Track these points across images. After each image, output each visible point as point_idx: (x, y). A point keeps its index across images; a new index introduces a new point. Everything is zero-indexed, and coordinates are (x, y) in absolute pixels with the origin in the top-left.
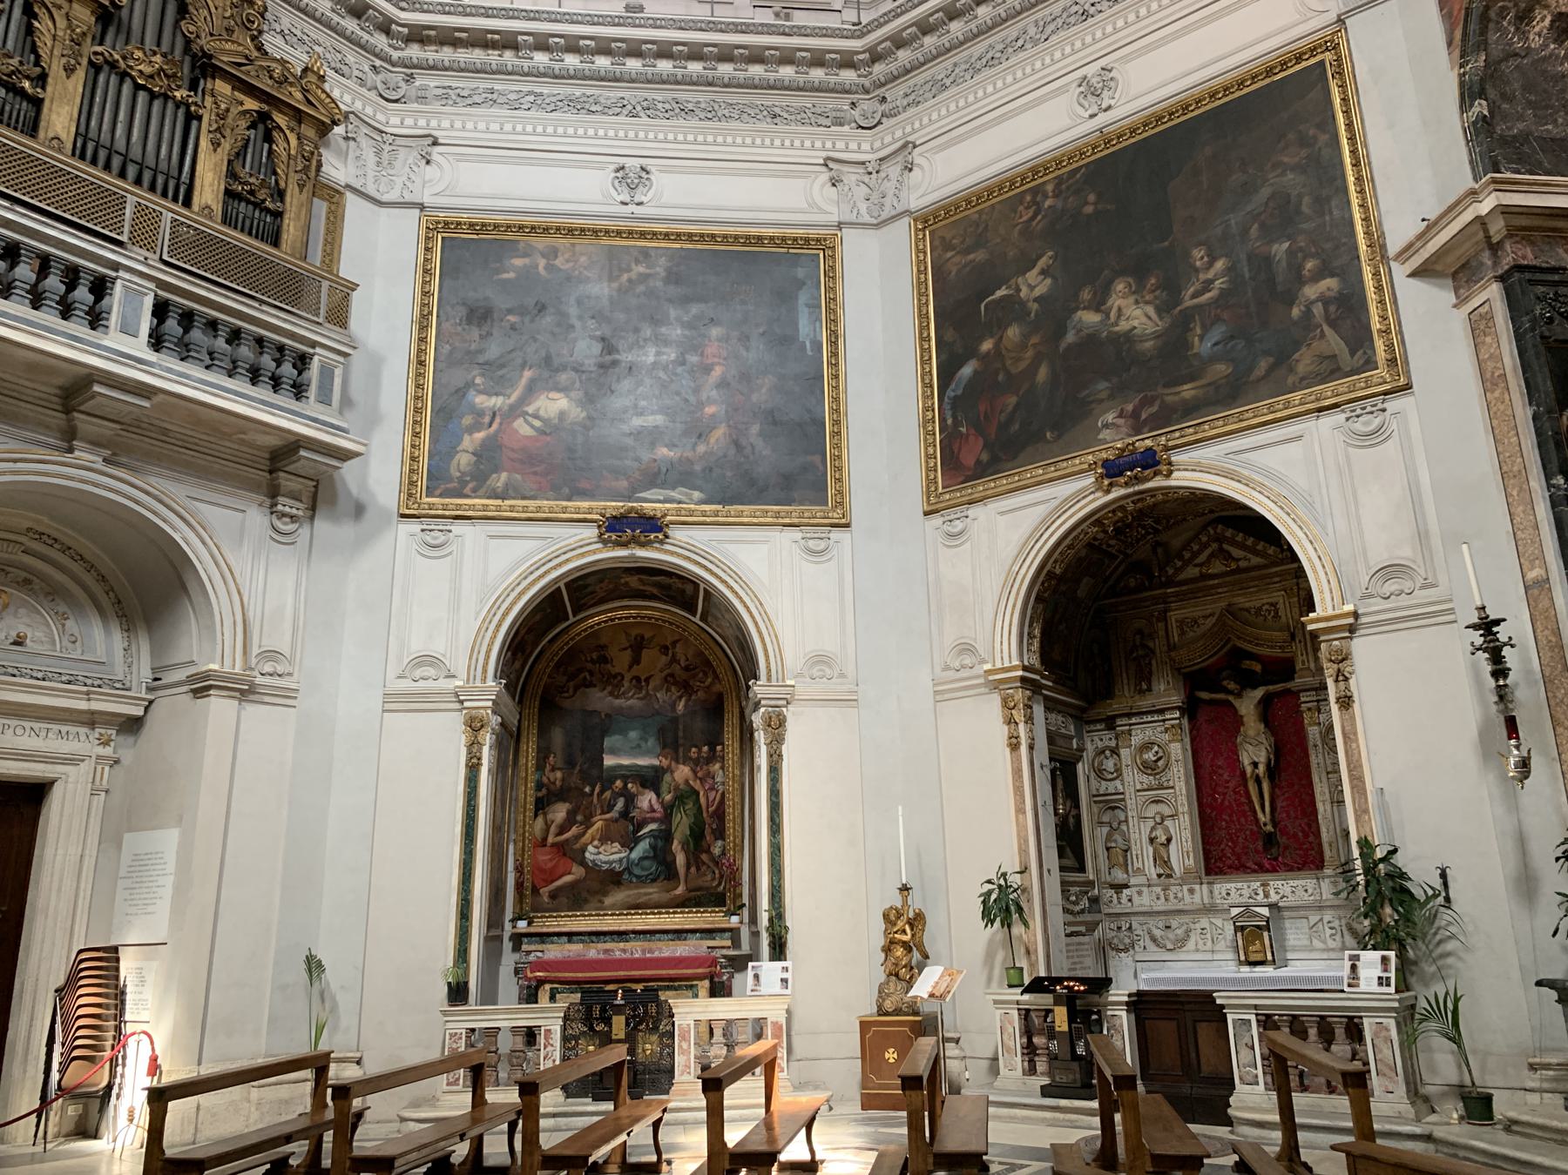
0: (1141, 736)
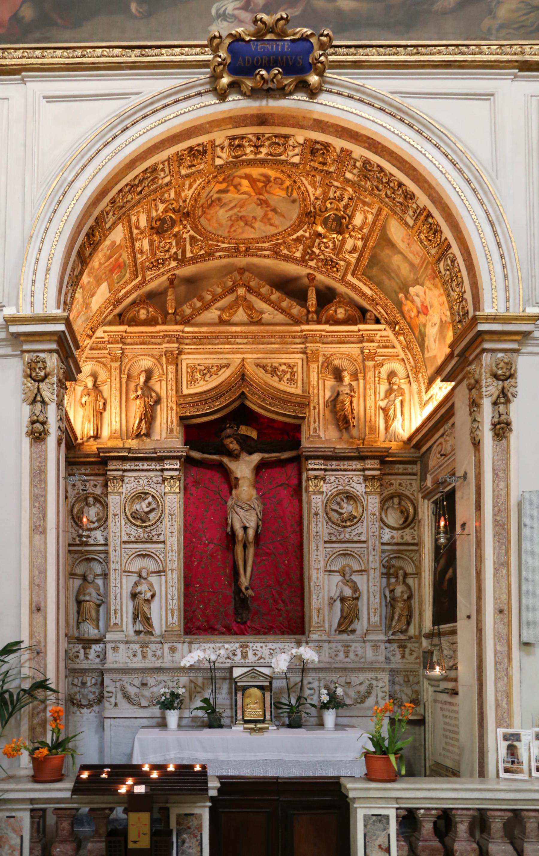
0: (134, 485)
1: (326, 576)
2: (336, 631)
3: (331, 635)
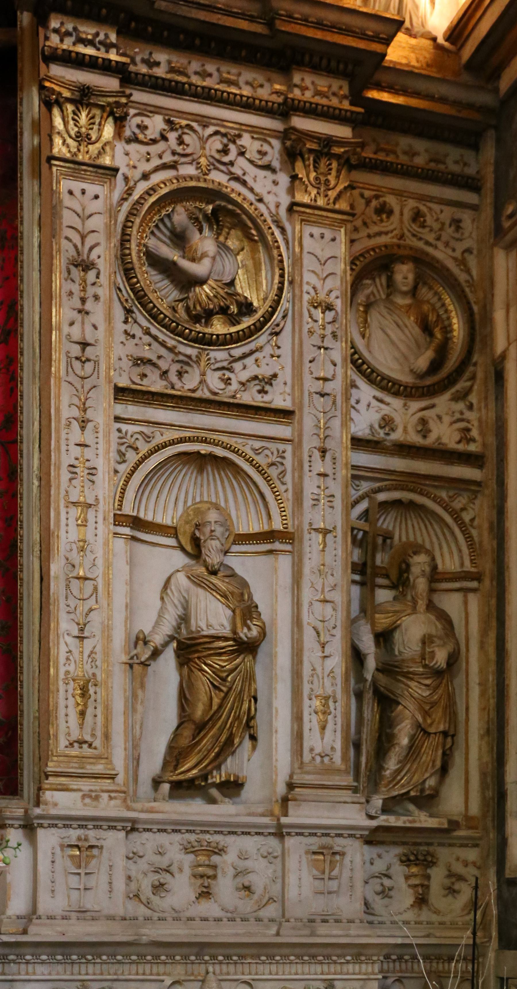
1: (120, 544)
2: (156, 783)
3: (135, 798)
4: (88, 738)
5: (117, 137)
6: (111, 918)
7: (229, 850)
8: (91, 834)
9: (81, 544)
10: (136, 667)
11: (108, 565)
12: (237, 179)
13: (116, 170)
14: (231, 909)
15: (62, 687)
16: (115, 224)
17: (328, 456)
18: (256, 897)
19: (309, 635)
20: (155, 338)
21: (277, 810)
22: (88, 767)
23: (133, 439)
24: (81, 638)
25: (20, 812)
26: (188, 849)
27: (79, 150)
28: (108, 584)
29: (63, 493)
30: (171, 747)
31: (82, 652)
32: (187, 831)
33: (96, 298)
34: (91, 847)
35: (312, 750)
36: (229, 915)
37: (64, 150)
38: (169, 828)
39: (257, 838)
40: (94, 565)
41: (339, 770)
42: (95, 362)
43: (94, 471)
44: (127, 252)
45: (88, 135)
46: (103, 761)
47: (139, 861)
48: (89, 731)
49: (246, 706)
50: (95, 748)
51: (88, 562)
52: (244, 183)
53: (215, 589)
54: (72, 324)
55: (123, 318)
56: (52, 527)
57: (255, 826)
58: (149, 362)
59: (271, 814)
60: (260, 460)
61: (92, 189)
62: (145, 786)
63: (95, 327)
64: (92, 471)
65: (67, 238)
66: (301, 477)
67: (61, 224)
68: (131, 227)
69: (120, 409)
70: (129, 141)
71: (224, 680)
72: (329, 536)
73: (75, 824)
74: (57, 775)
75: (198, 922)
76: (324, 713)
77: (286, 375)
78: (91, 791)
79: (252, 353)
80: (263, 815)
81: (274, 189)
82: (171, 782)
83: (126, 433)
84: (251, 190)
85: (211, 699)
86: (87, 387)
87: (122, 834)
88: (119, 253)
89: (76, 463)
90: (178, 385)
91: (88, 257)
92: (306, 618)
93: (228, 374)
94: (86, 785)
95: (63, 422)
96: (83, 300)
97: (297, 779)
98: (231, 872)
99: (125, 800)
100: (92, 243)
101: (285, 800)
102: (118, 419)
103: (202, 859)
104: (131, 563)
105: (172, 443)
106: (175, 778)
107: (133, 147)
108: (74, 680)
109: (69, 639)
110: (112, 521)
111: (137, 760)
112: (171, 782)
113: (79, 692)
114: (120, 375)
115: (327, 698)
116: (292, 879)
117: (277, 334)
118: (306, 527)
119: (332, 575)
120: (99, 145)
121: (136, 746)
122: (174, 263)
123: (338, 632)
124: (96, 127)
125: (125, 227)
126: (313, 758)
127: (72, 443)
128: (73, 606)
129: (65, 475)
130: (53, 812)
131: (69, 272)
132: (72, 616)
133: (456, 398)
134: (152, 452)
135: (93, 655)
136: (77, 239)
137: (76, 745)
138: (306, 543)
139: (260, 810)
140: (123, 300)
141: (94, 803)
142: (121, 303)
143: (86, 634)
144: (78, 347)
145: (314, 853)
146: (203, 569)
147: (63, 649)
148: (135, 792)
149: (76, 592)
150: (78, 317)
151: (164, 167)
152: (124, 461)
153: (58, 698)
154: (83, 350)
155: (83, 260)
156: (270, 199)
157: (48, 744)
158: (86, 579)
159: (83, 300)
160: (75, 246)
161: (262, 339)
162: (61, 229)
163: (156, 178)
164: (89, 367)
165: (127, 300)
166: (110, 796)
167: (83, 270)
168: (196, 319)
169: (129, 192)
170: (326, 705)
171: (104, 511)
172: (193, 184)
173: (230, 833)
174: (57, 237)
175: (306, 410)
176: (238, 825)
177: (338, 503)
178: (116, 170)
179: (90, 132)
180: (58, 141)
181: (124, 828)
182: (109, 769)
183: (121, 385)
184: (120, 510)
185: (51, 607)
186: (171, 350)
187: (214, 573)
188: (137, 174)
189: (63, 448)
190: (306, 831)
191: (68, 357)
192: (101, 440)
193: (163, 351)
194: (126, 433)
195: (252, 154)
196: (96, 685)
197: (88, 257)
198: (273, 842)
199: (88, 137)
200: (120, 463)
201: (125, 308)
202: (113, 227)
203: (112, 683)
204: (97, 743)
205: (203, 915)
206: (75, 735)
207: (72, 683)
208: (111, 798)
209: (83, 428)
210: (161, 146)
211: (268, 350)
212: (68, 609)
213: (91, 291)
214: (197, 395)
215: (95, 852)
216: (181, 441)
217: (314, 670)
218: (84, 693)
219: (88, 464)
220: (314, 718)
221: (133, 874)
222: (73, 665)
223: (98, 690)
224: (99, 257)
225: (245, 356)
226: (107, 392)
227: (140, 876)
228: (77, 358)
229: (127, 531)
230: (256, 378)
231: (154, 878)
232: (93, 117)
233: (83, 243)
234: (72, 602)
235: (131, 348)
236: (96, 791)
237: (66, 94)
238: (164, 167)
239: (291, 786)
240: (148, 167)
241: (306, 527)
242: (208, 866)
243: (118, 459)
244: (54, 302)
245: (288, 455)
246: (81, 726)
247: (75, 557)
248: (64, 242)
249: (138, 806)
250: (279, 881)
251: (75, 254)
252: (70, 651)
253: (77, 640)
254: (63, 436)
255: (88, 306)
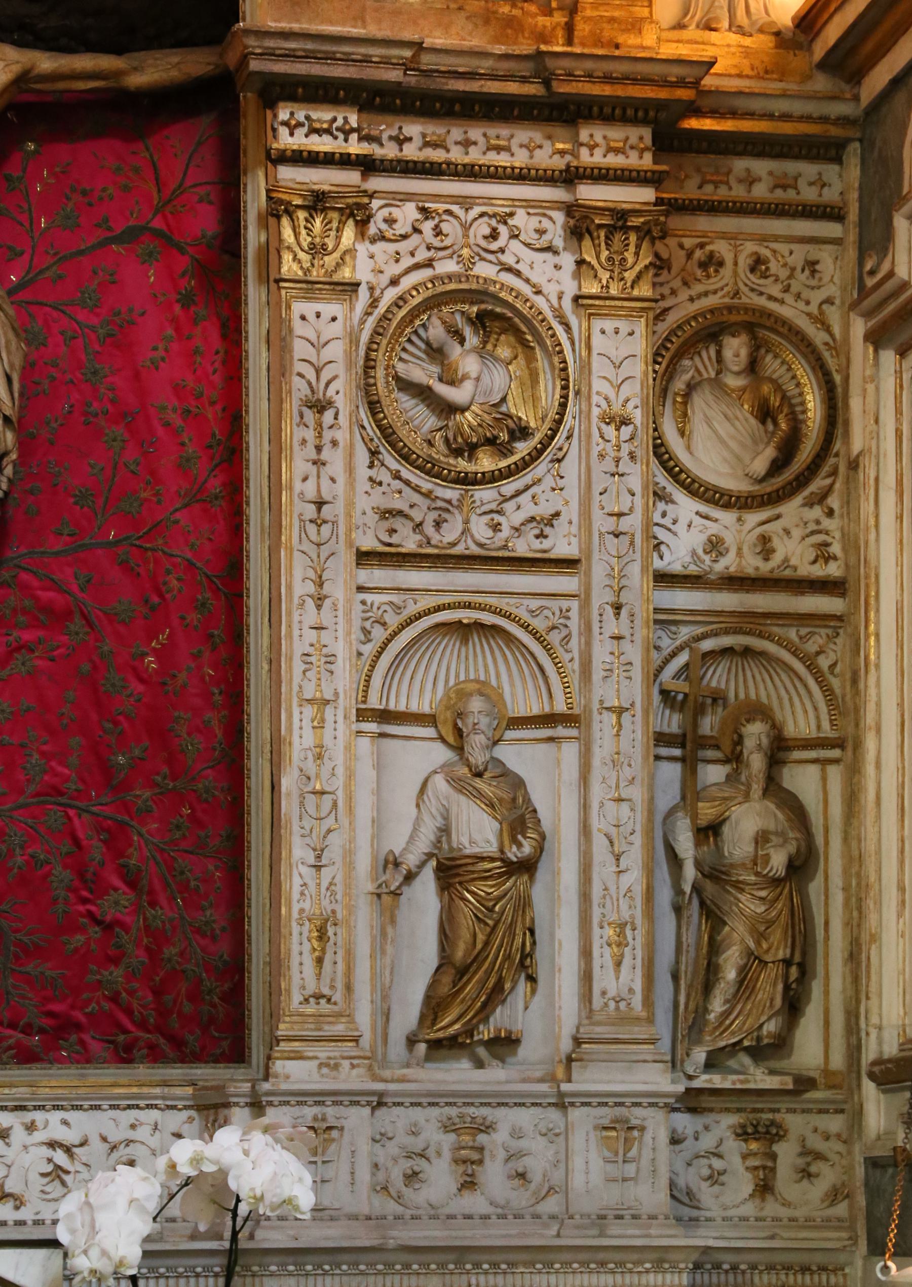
3: (385, 1063)
4: (326, 991)
5: (360, 236)
6: (354, 1217)
7: (499, 1126)
8: (330, 1111)
9: (318, 750)
10: (384, 897)
11: (350, 775)
12: (509, 270)
13: (358, 285)
14: (503, 1202)
15: (295, 929)
16: (357, 346)
17: (624, 612)
18: (533, 1186)
19: (599, 844)
20: (407, 483)
21: (560, 1073)
22: (326, 1027)
23: (380, 612)
24: (318, 868)
25: (246, 1087)
26: (448, 1127)
27: (313, 265)
28: (350, 798)
29: (295, 688)
30: (428, 998)
31: (319, 885)
32: (447, 1104)
33: (334, 443)
34: (330, 1128)
35: (604, 993)
36: (500, 1211)
37: (295, 267)
38: (424, 1100)
39: (533, 1110)
40: (333, 775)
41: (638, 1019)
42: (333, 523)
43: (332, 658)
44: (372, 381)
45: (324, 244)
46: (343, 1020)
47: (389, 1144)
48: (328, 981)
49: (518, 941)
50: (335, 1004)
51: (325, 772)
52: (518, 274)
53: (479, 795)
54: (305, 479)
55: (367, 462)
56: (283, 732)
57: (529, 1095)
58: (400, 513)
59: (551, 1078)
60: (538, 624)
61: (330, 309)
62: (397, 1048)
63: (333, 480)
64: (330, 659)
65: (300, 375)
66: (588, 644)
67: (292, 357)
68: (376, 351)
69: (365, 576)
70: (373, 241)
71: (491, 910)
72: (626, 717)
73: (310, 1100)
74: (290, 1039)
75: (460, 1221)
76: (619, 945)
77: (572, 512)
78: (329, 1058)
79: (527, 488)
80: (541, 1080)
81: (557, 274)
82: (427, 1042)
83: (372, 605)
84: (527, 281)
85: (475, 936)
86: (324, 553)
87: (367, 1111)
88: (362, 382)
89: (310, 650)
90: (435, 538)
91: (324, 395)
92: (596, 823)
93: (497, 517)
94: (323, 1052)
95: (296, 601)
96: (319, 449)
97: (584, 1032)
98: (501, 1155)
99: (370, 1068)
100: (330, 377)
101: (570, 1060)
102: (361, 589)
103: (466, 1139)
104: (379, 766)
105: (428, 612)
106: (433, 1036)
107: (381, 246)
108: (309, 920)
109: (304, 870)
110: (354, 718)
111: (387, 1016)
112: (427, 1042)
113: (316, 934)
114: (365, 533)
115: (622, 926)
116: (577, 1162)
117: (559, 461)
118: (596, 706)
119: (630, 765)
120: (336, 255)
121: (385, 997)
122: (429, 388)
123: (638, 840)
124: (333, 233)
125: (369, 349)
126: (606, 1004)
127: (305, 627)
128: (308, 827)
129: (298, 667)
130: (284, 1086)
131: (302, 416)
132: (308, 840)
133: (809, 503)
134: (402, 627)
135: (333, 887)
136: (311, 374)
137: (312, 1000)
138: (596, 726)
139: (538, 1074)
140: (367, 440)
141: (334, 1073)
142: (366, 444)
143: (324, 862)
144: (313, 507)
145: (605, 1128)
146: (466, 770)
147: (297, 881)
148: (385, 1055)
149: (311, 810)
150: (313, 469)
151: (417, 267)
152: (370, 641)
153: (290, 943)
154: (319, 510)
155: (318, 400)
156: (551, 290)
157: (280, 1002)
158: (323, 793)
159: (319, 449)
160: (309, 384)
161: (541, 468)
162: (292, 365)
163: (407, 282)
164: (326, 529)
165: (372, 440)
166: (352, 1064)
167: (318, 412)
168: (457, 453)
169: (374, 303)
170: (621, 934)
171: (345, 709)
172: (453, 286)
173: (499, 1105)
174: (287, 375)
175: (596, 556)
176: (510, 1095)
177: (637, 672)
178: (358, 285)
179: (326, 240)
180: (287, 257)
181: (369, 1103)
182: (351, 1030)
183: (364, 549)
184: (364, 702)
185: (283, 831)
186: (428, 495)
187: (479, 775)
188: (385, 280)
189: (296, 633)
190: (595, 1101)
191: (301, 520)
192: (341, 620)
193: (416, 498)
194: (372, 605)
195: (528, 235)
196: (335, 925)
197: (324, 395)
198: (554, 1115)
199: (324, 246)
200: (364, 643)
201: (369, 450)
202: (354, 354)
203: (356, 921)
204: (338, 997)
205: (467, 1211)
206: (311, 988)
207: (307, 923)
208: (353, 1066)
209: (319, 607)
210: (415, 239)
211: (549, 482)
212: (303, 831)
213: (328, 435)
214: (459, 550)
215: (335, 1134)
216: (438, 609)
217: (606, 889)
218: (322, 936)
219: (325, 651)
220: (607, 951)
221: (381, 1160)
222: (308, 901)
223: (339, 931)
224: (338, 393)
225: (518, 493)
226: (347, 557)
227: (390, 1164)
228: (311, 521)
229: (372, 727)
230: (532, 519)
231: (406, 1165)
232: (330, 222)
233: (318, 378)
234: (307, 823)
235: (378, 499)
236: (335, 1058)
237: (298, 201)
238: (417, 267)
239: (577, 1042)
240: (397, 269)
241: (596, 706)
242: (472, 1148)
243: (362, 638)
244: (283, 455)
245: (574, 614)
246: (319, 976)
247: (311, 767)
248: (296, 379)
249: (387, 1074)
250: (562, 1166)
251: (309, 392)
252: (305, 884)
253: (314, 870)
254: (296, 618)
255: (325, 455)
